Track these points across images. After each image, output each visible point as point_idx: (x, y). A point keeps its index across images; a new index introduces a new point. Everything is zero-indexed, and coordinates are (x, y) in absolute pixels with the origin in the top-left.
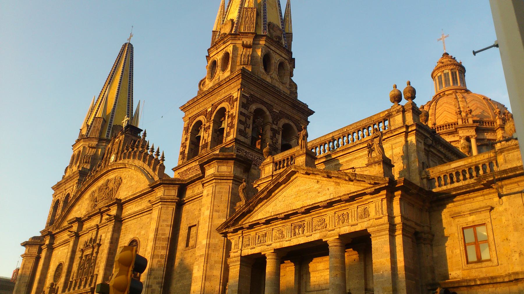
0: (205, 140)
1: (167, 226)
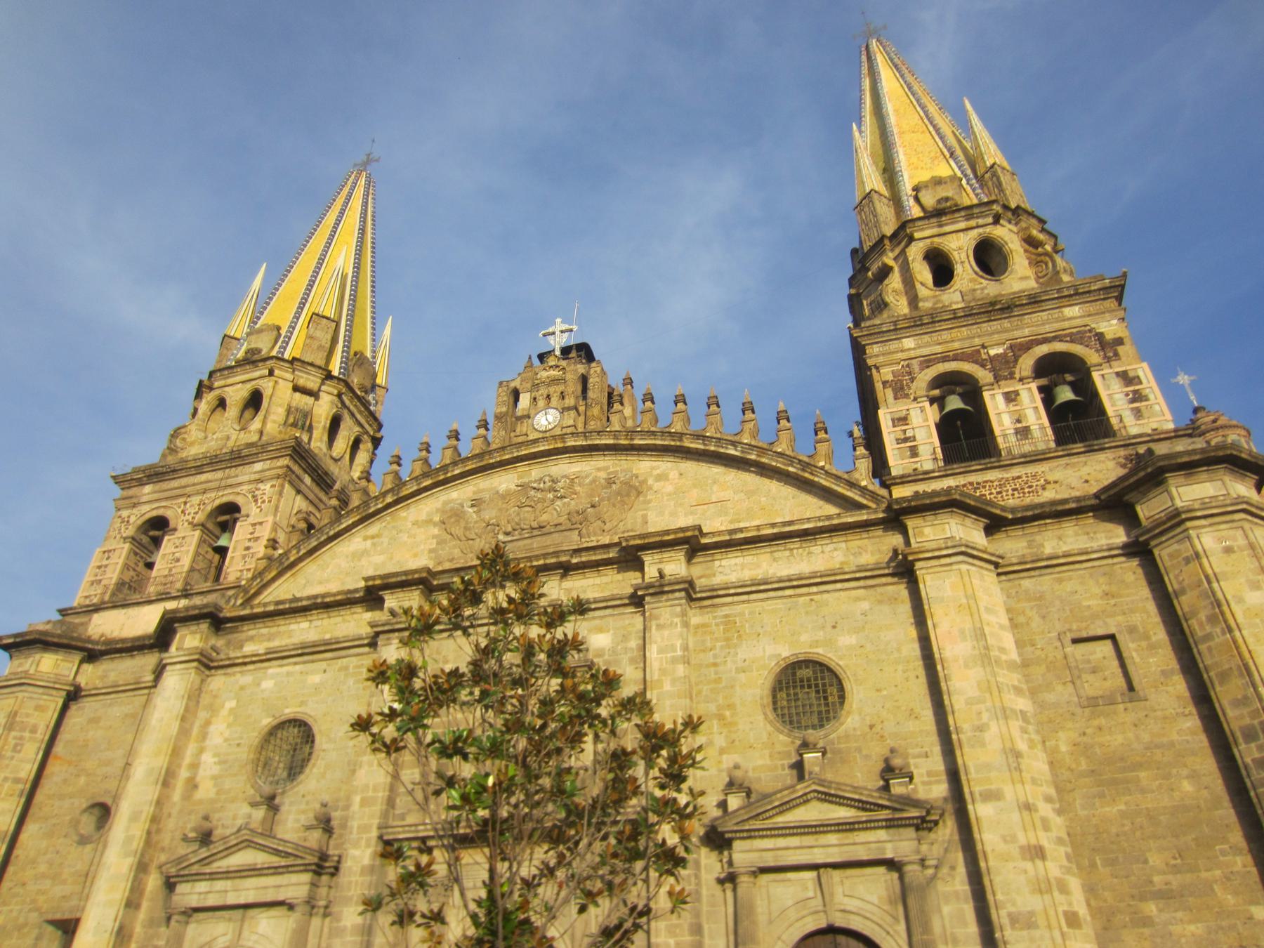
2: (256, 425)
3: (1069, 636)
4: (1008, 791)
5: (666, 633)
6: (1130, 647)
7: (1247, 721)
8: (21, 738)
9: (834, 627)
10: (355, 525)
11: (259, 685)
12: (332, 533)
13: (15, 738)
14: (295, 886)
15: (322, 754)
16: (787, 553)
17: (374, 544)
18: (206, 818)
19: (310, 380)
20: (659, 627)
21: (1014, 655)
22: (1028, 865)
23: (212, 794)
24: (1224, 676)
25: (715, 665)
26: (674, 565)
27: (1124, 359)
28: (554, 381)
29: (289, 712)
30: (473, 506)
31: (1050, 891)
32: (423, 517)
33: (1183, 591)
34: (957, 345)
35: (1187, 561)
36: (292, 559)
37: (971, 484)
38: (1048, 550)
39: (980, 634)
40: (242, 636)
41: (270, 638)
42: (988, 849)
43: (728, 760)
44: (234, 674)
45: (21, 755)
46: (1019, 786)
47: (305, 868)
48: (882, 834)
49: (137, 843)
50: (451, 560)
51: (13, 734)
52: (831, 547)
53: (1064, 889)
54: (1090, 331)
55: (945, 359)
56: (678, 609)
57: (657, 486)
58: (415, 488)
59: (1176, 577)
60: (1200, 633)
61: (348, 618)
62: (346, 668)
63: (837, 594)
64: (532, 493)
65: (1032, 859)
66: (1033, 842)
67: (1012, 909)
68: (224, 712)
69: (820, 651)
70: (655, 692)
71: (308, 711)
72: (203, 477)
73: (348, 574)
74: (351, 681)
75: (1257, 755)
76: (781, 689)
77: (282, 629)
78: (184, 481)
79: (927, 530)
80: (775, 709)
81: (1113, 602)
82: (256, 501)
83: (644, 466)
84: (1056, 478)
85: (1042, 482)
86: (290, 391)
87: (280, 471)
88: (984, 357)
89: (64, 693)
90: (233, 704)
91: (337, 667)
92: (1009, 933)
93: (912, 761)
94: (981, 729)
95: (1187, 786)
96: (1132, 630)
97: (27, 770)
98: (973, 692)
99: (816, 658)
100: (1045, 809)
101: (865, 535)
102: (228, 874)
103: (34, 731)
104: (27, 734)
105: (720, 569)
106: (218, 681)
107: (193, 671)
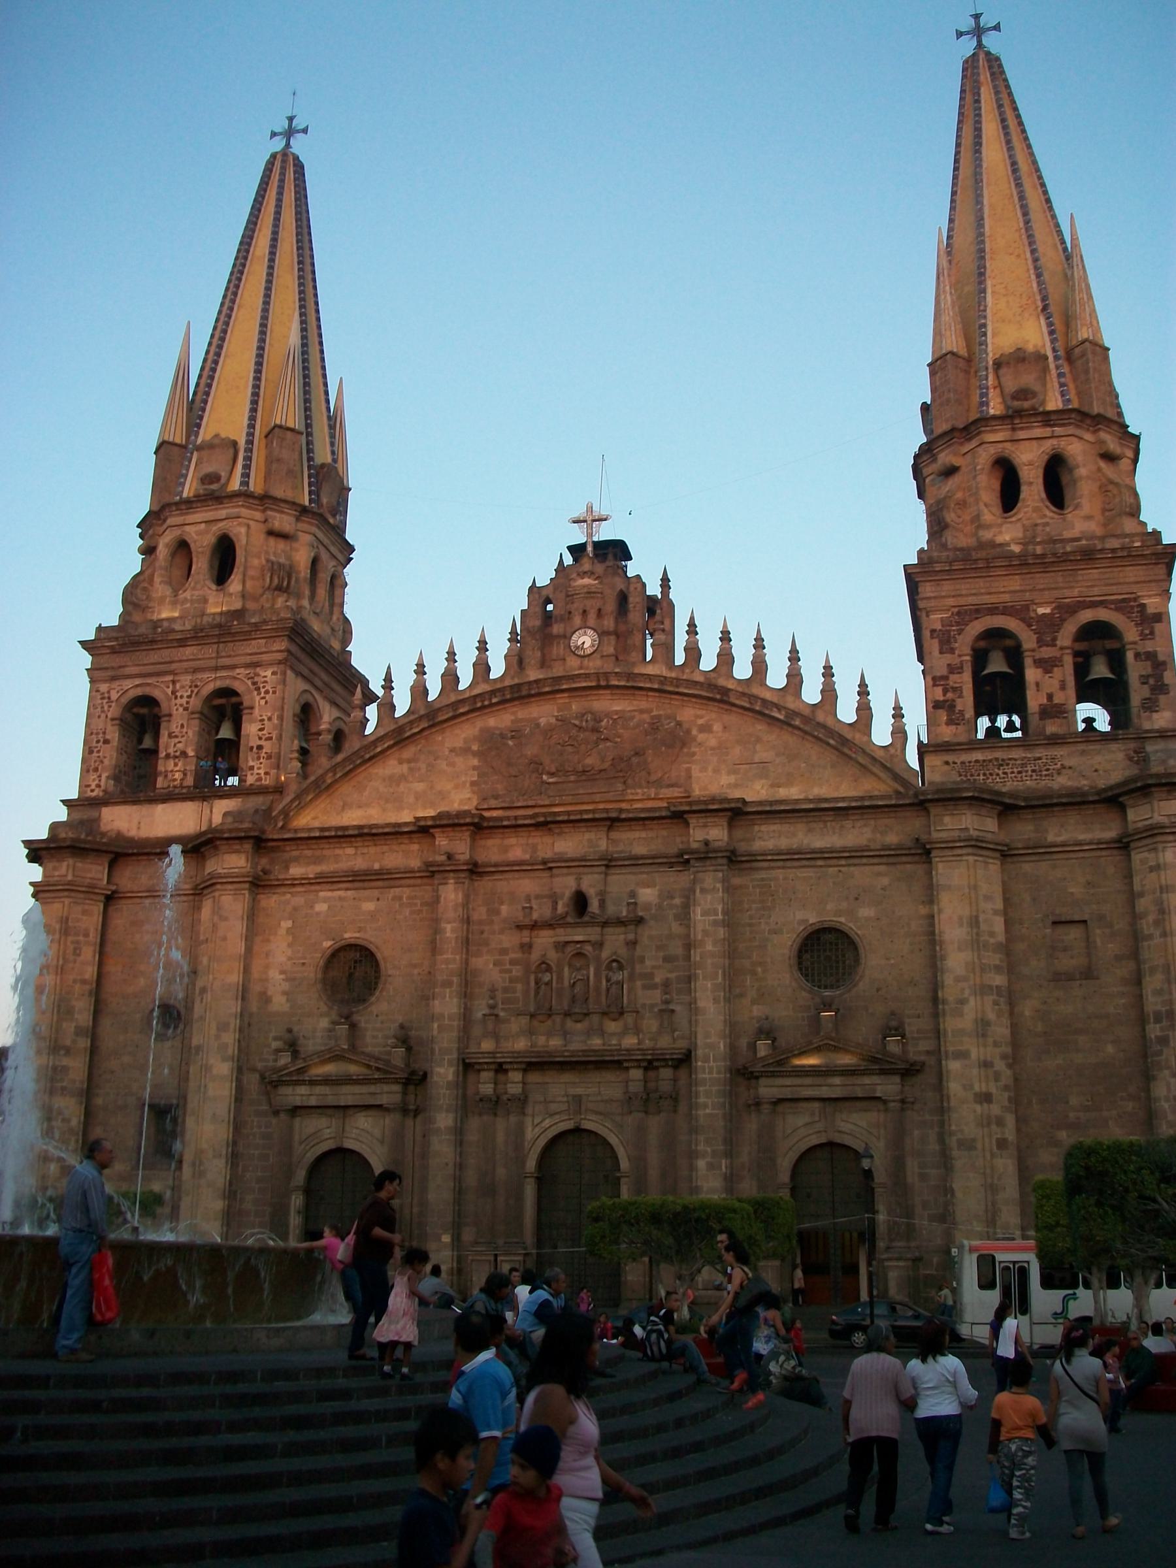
0: (1050, 697)
1: (996, 912)
2: (234, 585)
3: (1052, 918)
4: (974, 1054)
5: (709, 897)
6: (1098, 933)
7: (1159, 1007)
8: (78, 942)
9: (857, 899)
10: (389, 747)
11: (312, 907)
12: (367, 756)
13: (72, 942)
14: (389, 1094)
15: (390, 979)
16: (821, 825)
17: (411, 769)
18: (290, 1031)
19: (283, 521)
20: (703, 890)
21: (1001, 937)
22: (978, 1108)
23: (286, 1007)
24: (1153, 970)
25: (750, 925)
26: (717, 833)
27: (1157, 638)
28: (590, 593)
29: (349, 935)
30: (513, 737)
31: (989, 1124)
32: (459, 744)
33: (1141, 894)
34: (1006, 597)
35: (1152, 869)
36: (329, 781)
37: (997, 759)
38: (1051, 838)
39: (974, 922)
40: (286, 856)
41: (317, 860)
42: (952, 1095)
43: (757, 1011)
44: (284, 893)
45: (82, 958)
46: (982, 1049)
47: (396, 1081)
48: (876, 1079)
49: (232, 1050)
50: (496, 797)
51: (70, 939)
52: (858, 824)
53: (1000, 1122)
54: (1135, 599)
55: (993, 610)
56: (720, 874)
57: (701, 737)
58: (450, 714)
59: (1141, 880)
60: (1146, 932)
61: (394, 847)
62: (400, 898)
63: (863, 868)
64: (574, 732)
65: (981, 1103)
66: (984, 1090)
67: (960, 1136)
68: (282, 931)
69: (842, 920)
70: (698, 951)
71: (366, 936)
72: (188, 652)
73: (387, 801)
74: (407, 912)
75: (1158, 1034)
76: (806, 951)
77: (326, 852)
78: (166, 654)
79: (947, 819)
80: (800, 969)
81: (1092, 891)
82: (258, 689)
83: (688, 714)
84: (1071, 764)
85: (1059, 766)
86: (263, 536)
87: (280, 656)
88: (1033, 615)
89: (102, 898)
90: (289, 924)
91: (390, 896)
92: (955, 1153)
93: (907, 1020)
94: (962, 1002)
95: (1110, 1049)
96: (1101, 918)
97: (90, 972)
98: (960, 971)
99: (838, 926)
100: (1000, 1065)
101: (892, 815)
102: (327, 1081)
103: (86, 935)
104: (81, 938)
105: (760, 834)
106: (270, 901)
107: (246, 892)
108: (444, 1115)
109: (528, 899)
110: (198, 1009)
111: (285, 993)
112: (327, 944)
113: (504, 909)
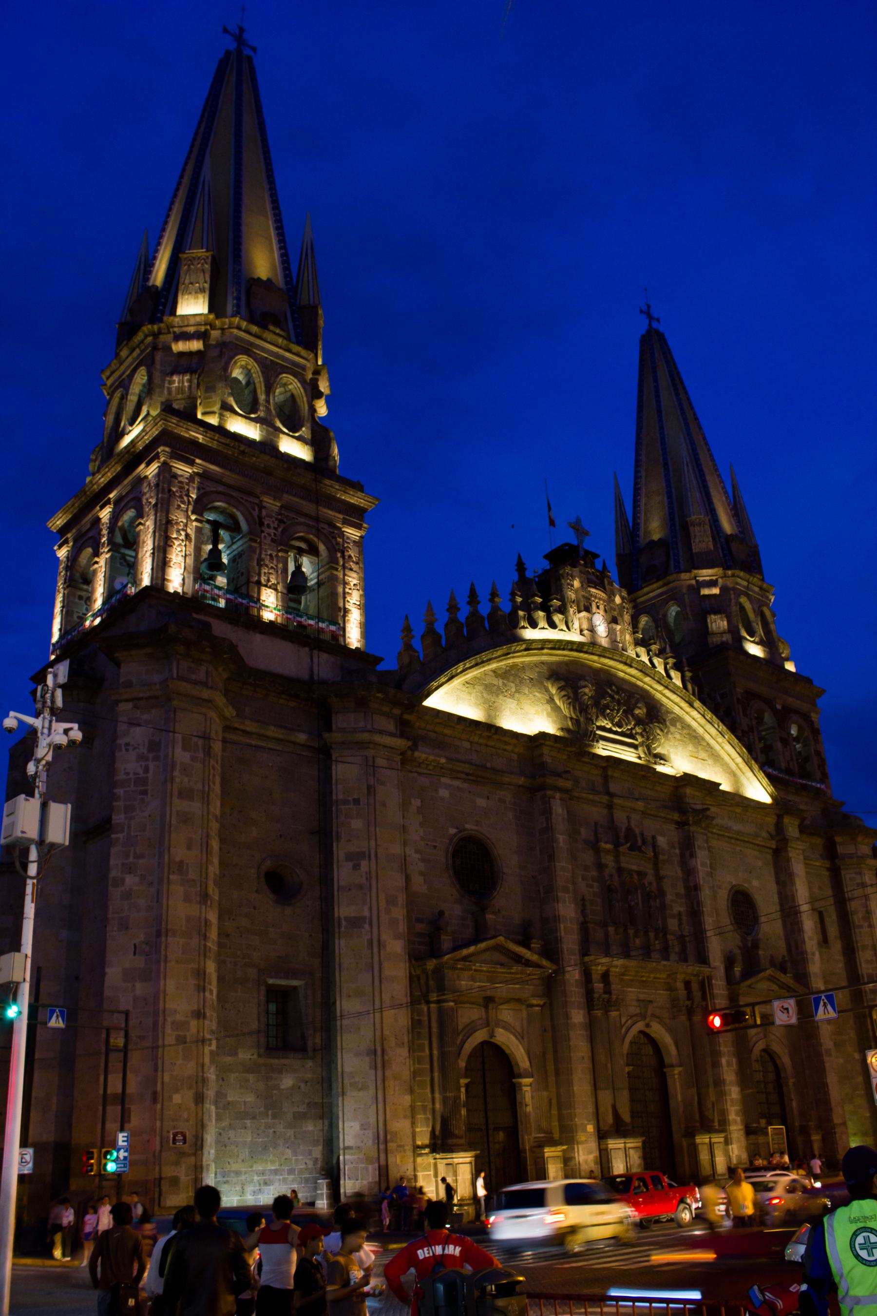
7: (870, 971)
94: (813, 954)
108: (576, 1011)
109: (596, 824)
110: (343, 874)
111: (421, 874)
112: (452, 831)
113: (583, 830)
